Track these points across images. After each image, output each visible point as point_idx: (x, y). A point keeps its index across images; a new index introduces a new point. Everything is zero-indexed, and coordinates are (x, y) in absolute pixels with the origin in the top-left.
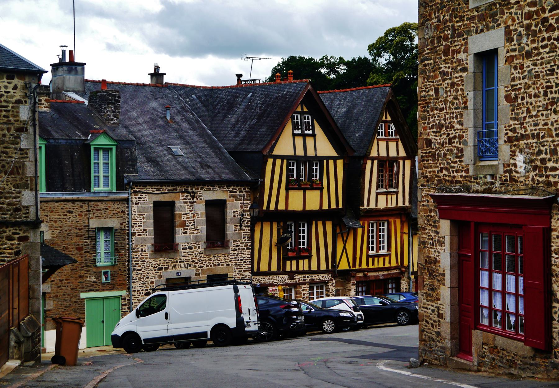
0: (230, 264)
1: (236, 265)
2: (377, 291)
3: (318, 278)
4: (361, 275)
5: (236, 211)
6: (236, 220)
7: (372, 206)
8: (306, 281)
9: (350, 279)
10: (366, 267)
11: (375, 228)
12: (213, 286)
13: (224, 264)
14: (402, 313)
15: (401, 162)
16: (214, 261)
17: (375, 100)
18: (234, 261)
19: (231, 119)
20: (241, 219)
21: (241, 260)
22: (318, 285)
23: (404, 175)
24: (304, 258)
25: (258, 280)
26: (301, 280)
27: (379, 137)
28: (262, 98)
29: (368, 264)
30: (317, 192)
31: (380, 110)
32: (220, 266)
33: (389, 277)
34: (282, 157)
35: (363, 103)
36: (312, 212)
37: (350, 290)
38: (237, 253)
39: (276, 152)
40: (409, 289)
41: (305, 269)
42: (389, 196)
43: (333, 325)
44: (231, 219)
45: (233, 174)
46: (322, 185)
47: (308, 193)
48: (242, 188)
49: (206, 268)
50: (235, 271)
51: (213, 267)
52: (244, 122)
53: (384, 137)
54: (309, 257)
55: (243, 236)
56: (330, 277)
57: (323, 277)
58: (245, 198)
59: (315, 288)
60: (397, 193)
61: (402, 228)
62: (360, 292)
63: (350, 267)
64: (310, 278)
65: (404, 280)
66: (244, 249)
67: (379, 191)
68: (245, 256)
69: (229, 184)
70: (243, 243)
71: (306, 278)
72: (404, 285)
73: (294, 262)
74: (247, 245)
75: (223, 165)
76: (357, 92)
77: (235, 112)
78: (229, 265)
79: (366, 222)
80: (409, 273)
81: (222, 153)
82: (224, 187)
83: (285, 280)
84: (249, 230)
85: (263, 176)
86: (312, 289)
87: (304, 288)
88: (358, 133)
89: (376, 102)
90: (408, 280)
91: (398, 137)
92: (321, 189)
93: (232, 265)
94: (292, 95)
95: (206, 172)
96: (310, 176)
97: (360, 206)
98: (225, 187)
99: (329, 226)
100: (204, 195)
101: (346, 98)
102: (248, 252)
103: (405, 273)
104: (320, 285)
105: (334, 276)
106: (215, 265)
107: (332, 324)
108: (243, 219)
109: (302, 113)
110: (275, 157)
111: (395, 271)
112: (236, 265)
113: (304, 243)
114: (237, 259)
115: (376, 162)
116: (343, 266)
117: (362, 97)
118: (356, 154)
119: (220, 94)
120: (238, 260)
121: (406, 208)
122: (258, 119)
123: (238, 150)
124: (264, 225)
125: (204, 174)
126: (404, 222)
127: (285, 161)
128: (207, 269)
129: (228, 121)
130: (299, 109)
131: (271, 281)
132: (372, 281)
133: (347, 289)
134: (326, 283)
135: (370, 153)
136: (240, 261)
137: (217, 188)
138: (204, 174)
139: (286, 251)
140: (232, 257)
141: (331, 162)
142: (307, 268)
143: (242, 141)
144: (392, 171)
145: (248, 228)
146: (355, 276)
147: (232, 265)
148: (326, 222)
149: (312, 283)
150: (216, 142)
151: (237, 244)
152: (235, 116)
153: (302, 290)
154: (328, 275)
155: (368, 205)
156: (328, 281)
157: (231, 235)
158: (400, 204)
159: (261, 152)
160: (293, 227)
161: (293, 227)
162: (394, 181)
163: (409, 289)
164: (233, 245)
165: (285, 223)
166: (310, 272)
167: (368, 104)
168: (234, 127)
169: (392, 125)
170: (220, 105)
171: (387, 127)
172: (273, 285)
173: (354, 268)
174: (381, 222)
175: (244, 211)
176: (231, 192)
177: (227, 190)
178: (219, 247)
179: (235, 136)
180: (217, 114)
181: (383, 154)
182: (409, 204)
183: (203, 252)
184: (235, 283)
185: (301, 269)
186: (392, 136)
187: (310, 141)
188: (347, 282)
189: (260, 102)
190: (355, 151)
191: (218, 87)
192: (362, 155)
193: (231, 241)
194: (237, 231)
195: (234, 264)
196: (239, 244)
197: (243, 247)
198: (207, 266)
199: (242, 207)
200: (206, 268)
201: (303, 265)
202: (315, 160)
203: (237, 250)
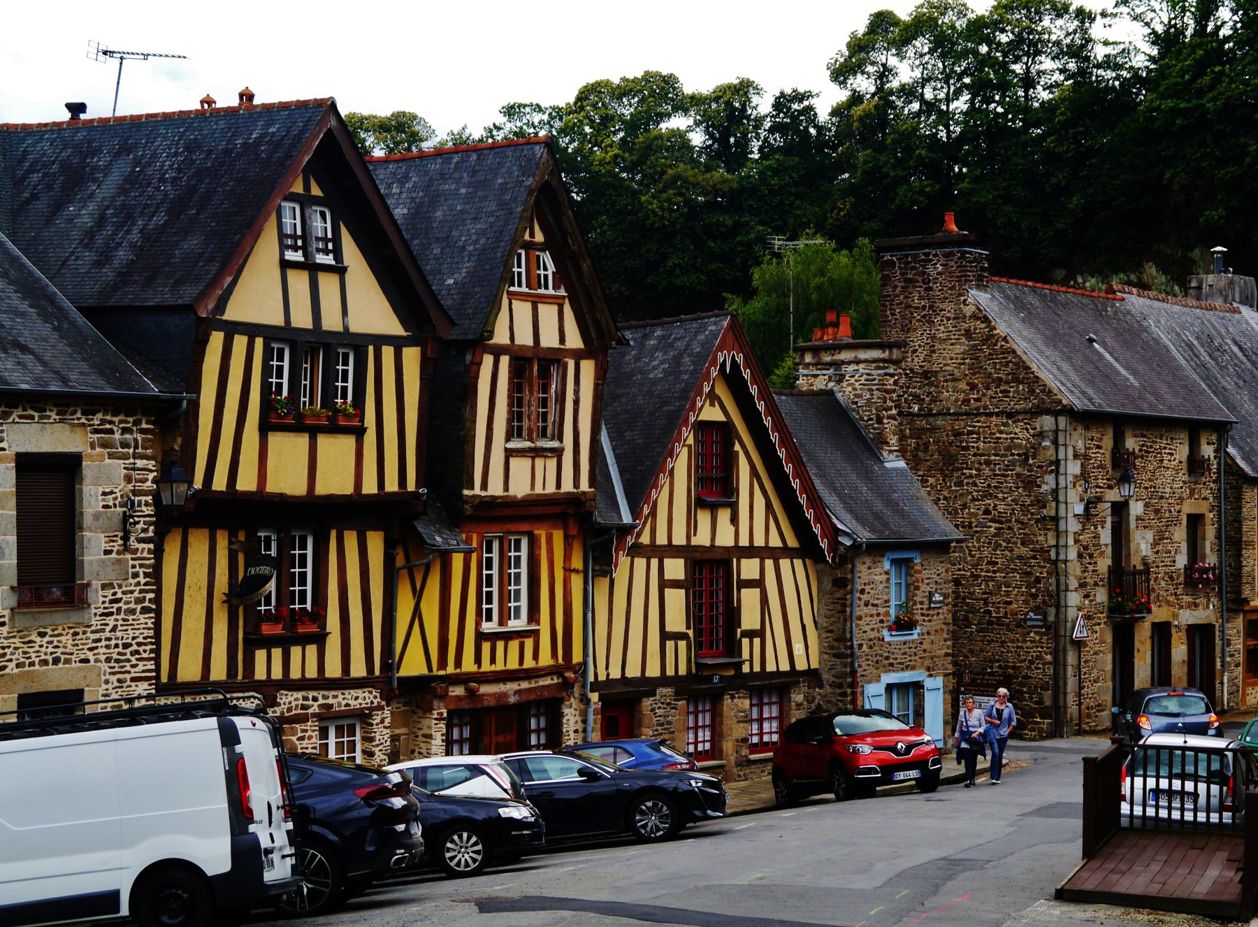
0: (92, 658)
1: (108, 660)
2: (500, 739)
3: (344, 703)
4: (458, 691)
5: (112, 493)
6: (110, 519)
7: (495, 489)
8: (310, 711)
9: (432, 703)
10: (474, 668)
11: (495, 555)
12: (141, 724)
13: (73, 657)
14: (649, 804)
15: (571, 364)
16: (41, 647)
17: (500, 181)
18: (104, 650)
19: (78, 216)
20: (125, 518)
21: (126, 646)
22: (340, 723)
23: (576, 402)
24: (304, 641)
26: (297, 706)
27: (512, 289)
28: (176, 154)
29: (478, 660)
30: (349, 442)
31: (519, 209)
32: (61, 665)
33: (533, 697)
34: (252, 330)
35: (463, 191)
36: (332, 501)
37: (429, 736)
38: (112, 623)
39: (232, 313)
40: (585, 731)
41: (308, 676)
42: (539, 462)
43: (479, 847)
44: (97, 516)
45: (101, 374)
46: (362, 420)
47: (323, 441)
48: (131, 419)
49: (16, 671)
50: (107, 682)
51: (37, 667)
52: (123, 224)
53: (524, 289)
54: (320, 639)
55: (131, 570)
57: (357, 698)
58: (140, 450)
59: (332, 733)
60: (558, 453)
61: (567, 557)
62: (456, 741)
63: (430, 669)
64: (321, 701)
65: (571, 707)
66: (133, 612)
67: (511, 445)
68: (137, 632)
69: (90, 404)
70: (132, 592)
71: (311, 702)
72: (571, 718)
73: (277, 653)
74: (143, 600)
75: (70, 345)
76: (439, 161)
77: (92, 195)
78: (86, 661)
79: (475, 537)
80: (583, 686)
81: (62, 313)
82: (74, 413)
84: (149, 551)
85: (196, 386)
86: (324, 734)
87: (303, 731)
88: (451, 274)
89: (503, 189)
90: (582, 707)
91: (562, 292)
92: (359, 432)
93: (97, 661)
94: (279, 144)
95: (19, 363)
96: (329, 392)
97: (462, 488)
98: (79, 415)
99: (376, 543)
100: (12, 437)
101: (406, 177)
102: (147, 620)
103: (573, 687)
104: (345, 722)
105: (388, 697)
106: (45, 662)
107: (475, 844)
108: (132, 517)
109: (305, 201)
110: (232, 329)
111: (546, 681)
112: (108, 660)
113: (303, 594)
114: (113, 642)
115: (505, 360)
116: (413, 665)
117: (457, 175)
118: (454, 335)
119: (34, 145)
120: (117, 646)
121: (583, 498)
122: (170, 213)
123: (111, 302)
124: (191, 539)
125: (13, 370)
126: (573, 537)
127: (259, 342)
128: (19, 675)
129: (70, 221)
130: (298, 188)
132: (489, 710)
133: (420, 733)
134: (363, 716)
135: (491, 334)
136: (120, 649)
137: (54, 416)
138: (13, 370)
139: (255, 620)
140: (97, 636)
141: (388, 352)
142: (312, 673)
143: (124, 277)
144: (546, 389)
145: (146, 546)
146: (443, 697)
147: (97, 661)
148: (368, 533)
149: (326, 716)
150: (38, 280)
151: (115, 594)
152: (91, 207)
153: (299, 739)
154: (370, 692)
155: (484, 486)
156: (371, 709)
157: (96, 567)
158: (567, 486)
159: (190, 309)
160: (274, 545)
161: (274, 545)
162: (551, 418)
163: (585, 731)
164: (102, 599)
165: (251, 534)
166: (323, 683)
167: (480, 193)
168: (92, 238)
169: (547, 258)
170: (35, 177)
171: (534, 260)
173: (442, 673)
174: (513, 538)
175: (135, 493)
176: (96, 431)
177: (83, 425)
178: (56, 603)
179: (98, 264)
180: (28, 202)
181: (524, 338)
182: (590, 487)
183: (6, 619)
184: (222, 711)
185: (295, 674)
186: (546, 288)
187: (328, 284)
188: (420, 713)
189: (171, 166)
190: (453, 324)
191: (25, 126)
192: (470, 337)
193: (96, 584)
194: (114, 555)
195: (103, 658)
196: (119, 595)
197: (132, 606)
198: (18, 666)
199: (128, 479)
200: (16, 671)
201: (303, 662)
202: (343, 345)
203: (112, 614)
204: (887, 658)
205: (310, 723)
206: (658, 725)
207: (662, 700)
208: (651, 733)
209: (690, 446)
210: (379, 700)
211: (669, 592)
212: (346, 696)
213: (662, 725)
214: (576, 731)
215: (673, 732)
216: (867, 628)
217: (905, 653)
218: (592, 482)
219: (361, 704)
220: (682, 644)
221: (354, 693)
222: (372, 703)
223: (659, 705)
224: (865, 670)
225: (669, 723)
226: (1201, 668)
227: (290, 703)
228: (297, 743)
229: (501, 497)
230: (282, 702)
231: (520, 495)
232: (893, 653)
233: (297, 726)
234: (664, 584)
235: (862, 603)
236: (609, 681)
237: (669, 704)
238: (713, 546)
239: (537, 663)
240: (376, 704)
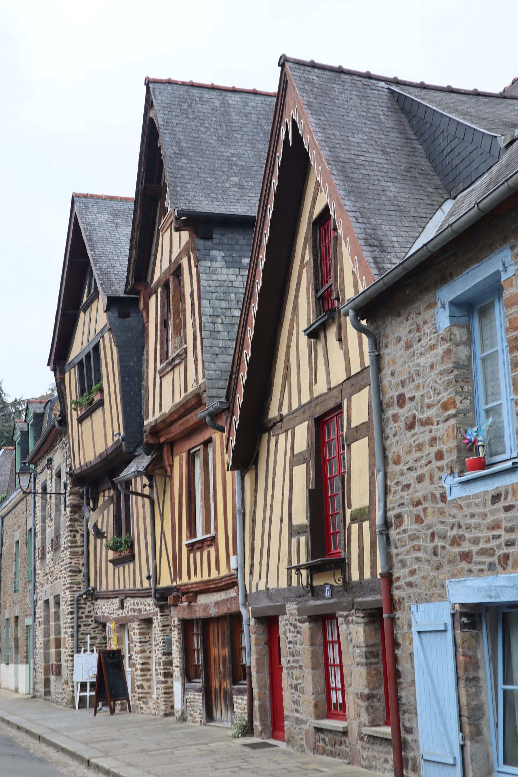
204: (455, 541)
216: (410, 478)
217: (496, 526)
224: (413, 573)
226: (327, 468)
232: (468, 528)
235: (401, 424)
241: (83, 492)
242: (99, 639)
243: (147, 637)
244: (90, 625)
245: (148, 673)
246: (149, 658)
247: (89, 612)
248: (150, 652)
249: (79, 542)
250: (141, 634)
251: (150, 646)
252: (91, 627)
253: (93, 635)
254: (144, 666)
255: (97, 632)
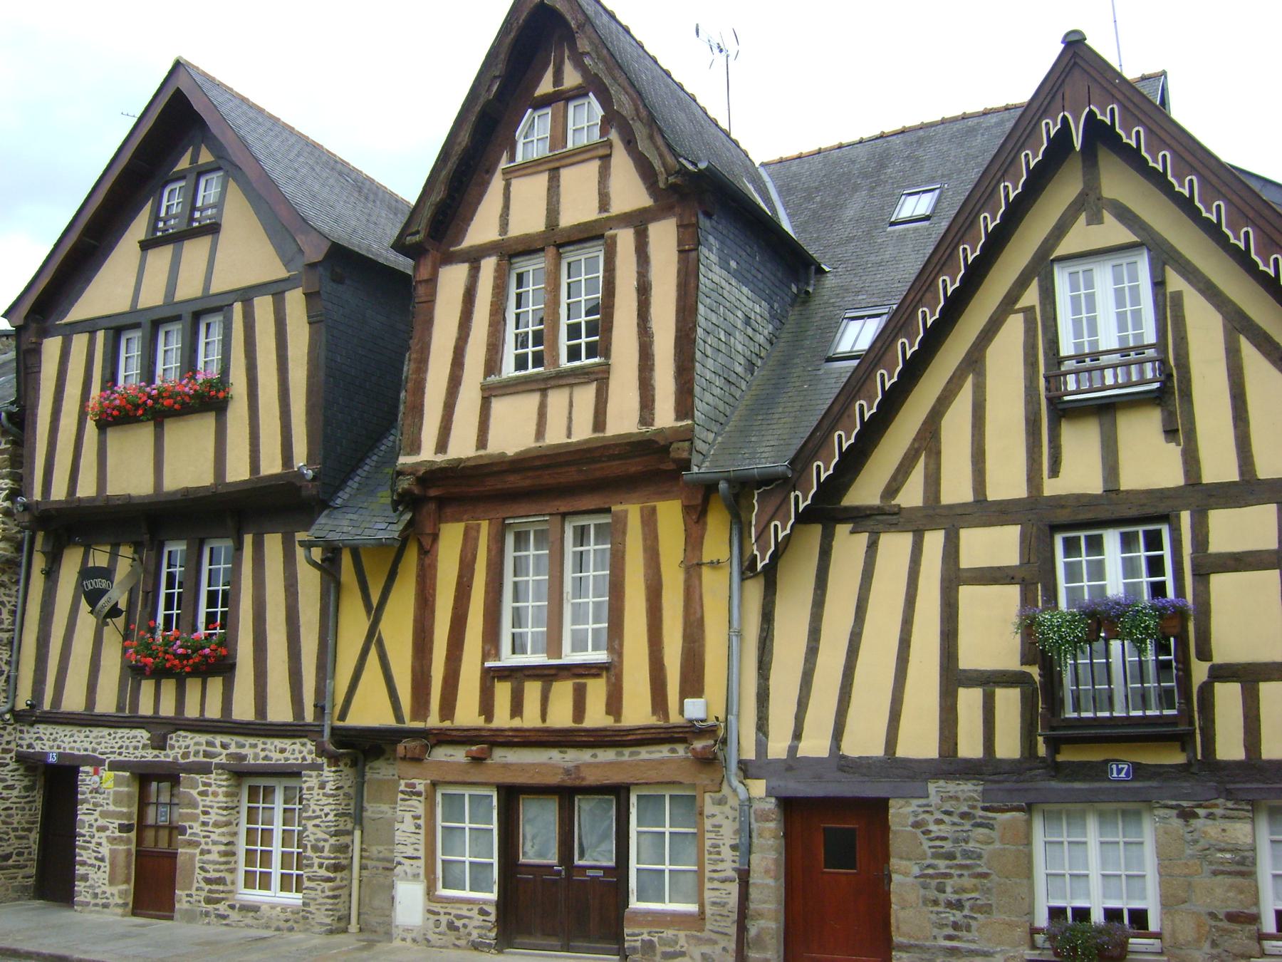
3: (262, 754)
7: (462, 447)
10: (479, 722)
15: (625, 239)
23: (644, 290)
25: (55, 740)
26: (196, 754)
29: (487, 708)
56: (310, 752)
61: (694, 541)
63: (399, 718)
64: (233, 749)
65: (721, 802)
71: (219, 749)
83: (136, 748)
87: (205, 784)
115: (489, 266)
127: (100, 335)
131: (90, 747)
142: (214, 711)
149: (240, 773)
154: (304, 745)
155: (442, 446)
172: (96, 763)
205: (213, 776)
206: (935, 856)
207: (947, 807)
208: (916, 870)
209: (1029, 311)
210: (314, 755)
211: (967, 594)
212: (268, 746)
213: (951, 856)
214: (734, 847)
215: (985, 875)
218: (684, 406)
219: (287, 759)
220: (1009, 701)
221: (278, 743)
222: (304, 759)
223: (939, 816)
225: (966, 854)
227: (187, 747)
228: (199, 798)
229: (468, 459)
230: (177, 745)
231: (511, 452)
233: (198, 777)
234: (953, 577)
236: (793, 763)
237: (964, 815)
238: (1112, 490)
239: (618, 719)
240: (309, 761)
241: (23, 539)
242: (18, 790)
243: (236, 799)
244: (8, 764)
245: (232, 859)
246: (235, 834)
247: (8, 743)
248: (237, 825)
249: (6, 622)
250: (227, 795)
251: (238, 815)
252: (8, 768)
253: (10, 783)
254: (228, 848)
255: (16, 778)
